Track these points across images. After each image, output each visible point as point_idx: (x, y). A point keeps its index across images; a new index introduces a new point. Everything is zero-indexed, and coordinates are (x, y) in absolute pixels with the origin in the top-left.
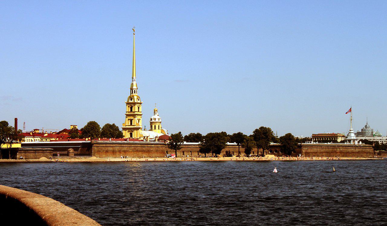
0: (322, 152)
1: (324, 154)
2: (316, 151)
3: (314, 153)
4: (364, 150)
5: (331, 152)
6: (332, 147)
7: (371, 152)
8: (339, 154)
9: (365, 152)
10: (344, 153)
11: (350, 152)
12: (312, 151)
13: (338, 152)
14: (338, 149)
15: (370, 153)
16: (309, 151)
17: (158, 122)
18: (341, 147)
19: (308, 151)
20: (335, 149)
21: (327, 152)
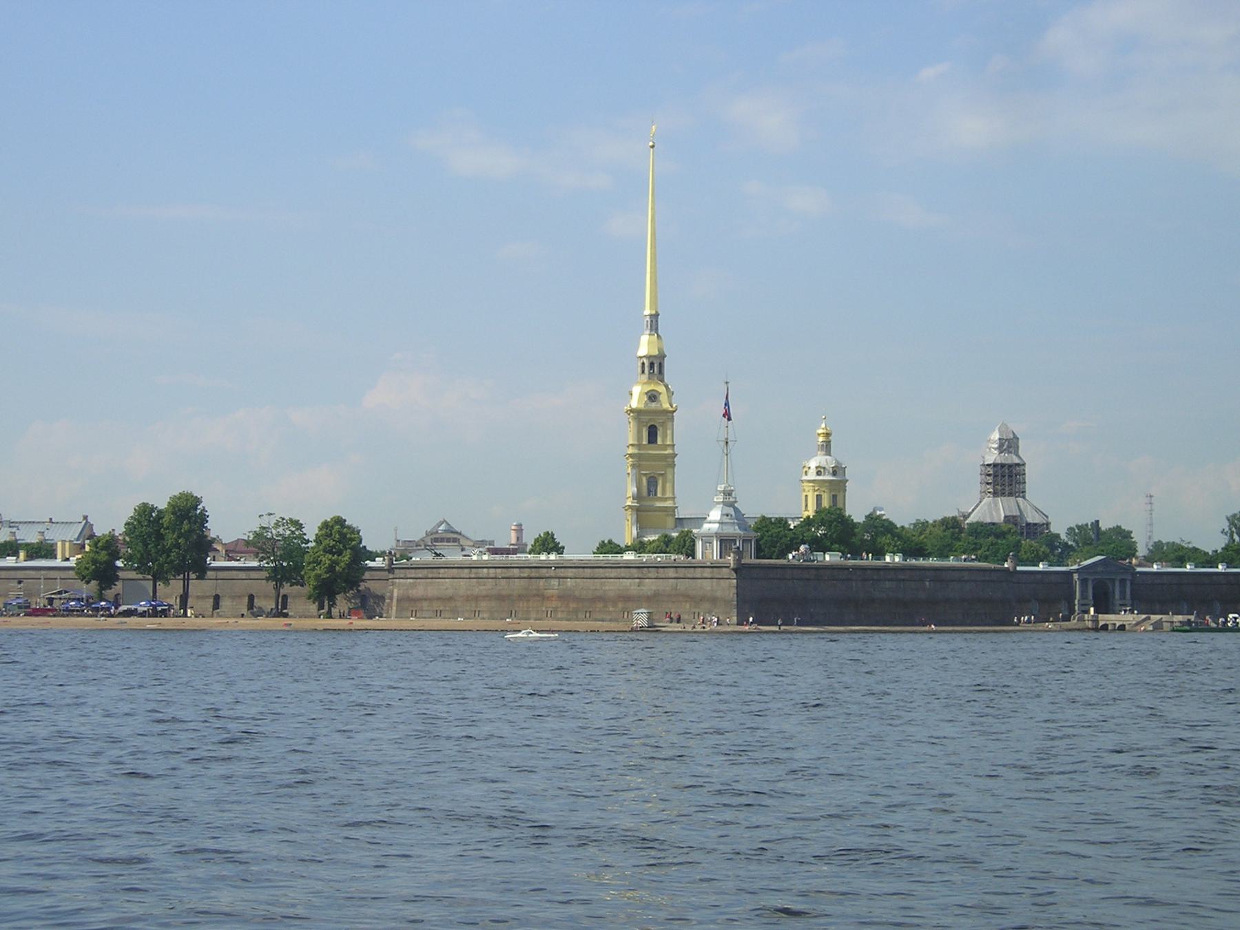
0: (477, 598)
1: (483, 605)
2: (450, 592)
3: (438, 599)
4: (683, 585)
5: (520, 597)
6: (526, 573)
7: (719, 594)
8: (554, 604)
9: (688, 597)
10: (578, 599)
11: (611, 594)
12: (432, 591)
13: (549, 598)
14: (555, 582)
15: (714, 600)
16: (420, 590)
17: (813, 481)
18: (570, 573)
19: (414, 593)
20: (542, 582)
21: (500, 598)
